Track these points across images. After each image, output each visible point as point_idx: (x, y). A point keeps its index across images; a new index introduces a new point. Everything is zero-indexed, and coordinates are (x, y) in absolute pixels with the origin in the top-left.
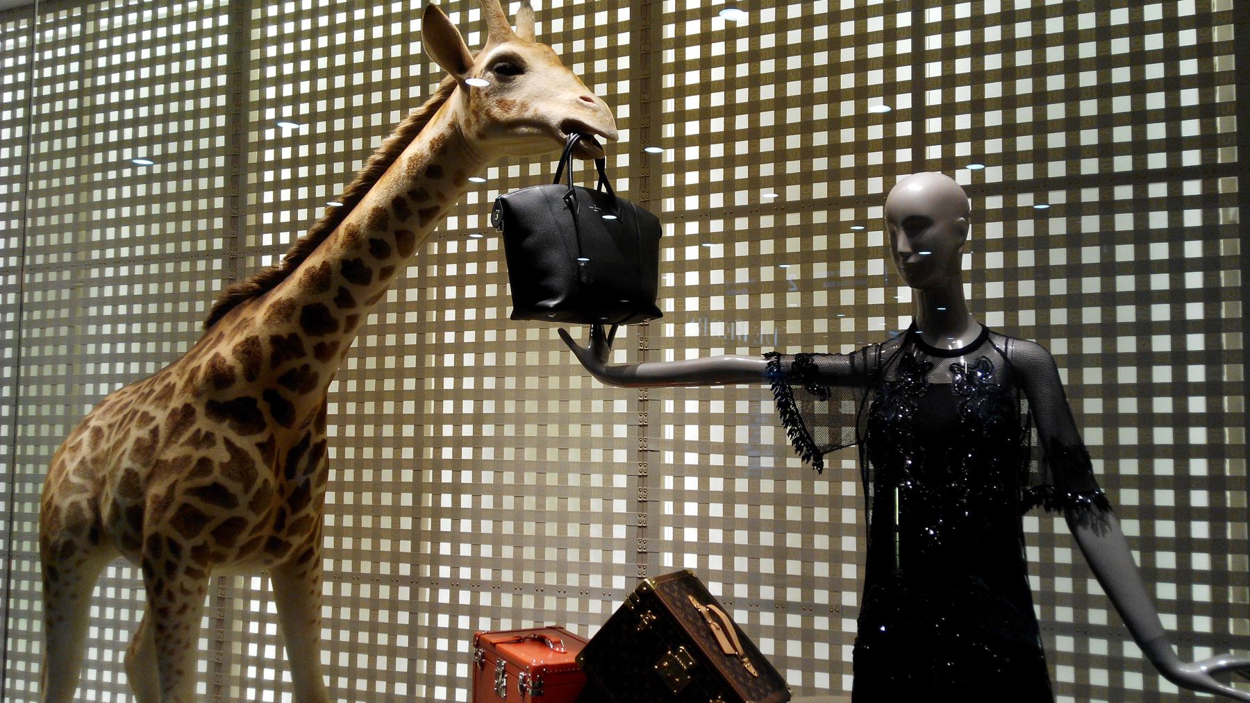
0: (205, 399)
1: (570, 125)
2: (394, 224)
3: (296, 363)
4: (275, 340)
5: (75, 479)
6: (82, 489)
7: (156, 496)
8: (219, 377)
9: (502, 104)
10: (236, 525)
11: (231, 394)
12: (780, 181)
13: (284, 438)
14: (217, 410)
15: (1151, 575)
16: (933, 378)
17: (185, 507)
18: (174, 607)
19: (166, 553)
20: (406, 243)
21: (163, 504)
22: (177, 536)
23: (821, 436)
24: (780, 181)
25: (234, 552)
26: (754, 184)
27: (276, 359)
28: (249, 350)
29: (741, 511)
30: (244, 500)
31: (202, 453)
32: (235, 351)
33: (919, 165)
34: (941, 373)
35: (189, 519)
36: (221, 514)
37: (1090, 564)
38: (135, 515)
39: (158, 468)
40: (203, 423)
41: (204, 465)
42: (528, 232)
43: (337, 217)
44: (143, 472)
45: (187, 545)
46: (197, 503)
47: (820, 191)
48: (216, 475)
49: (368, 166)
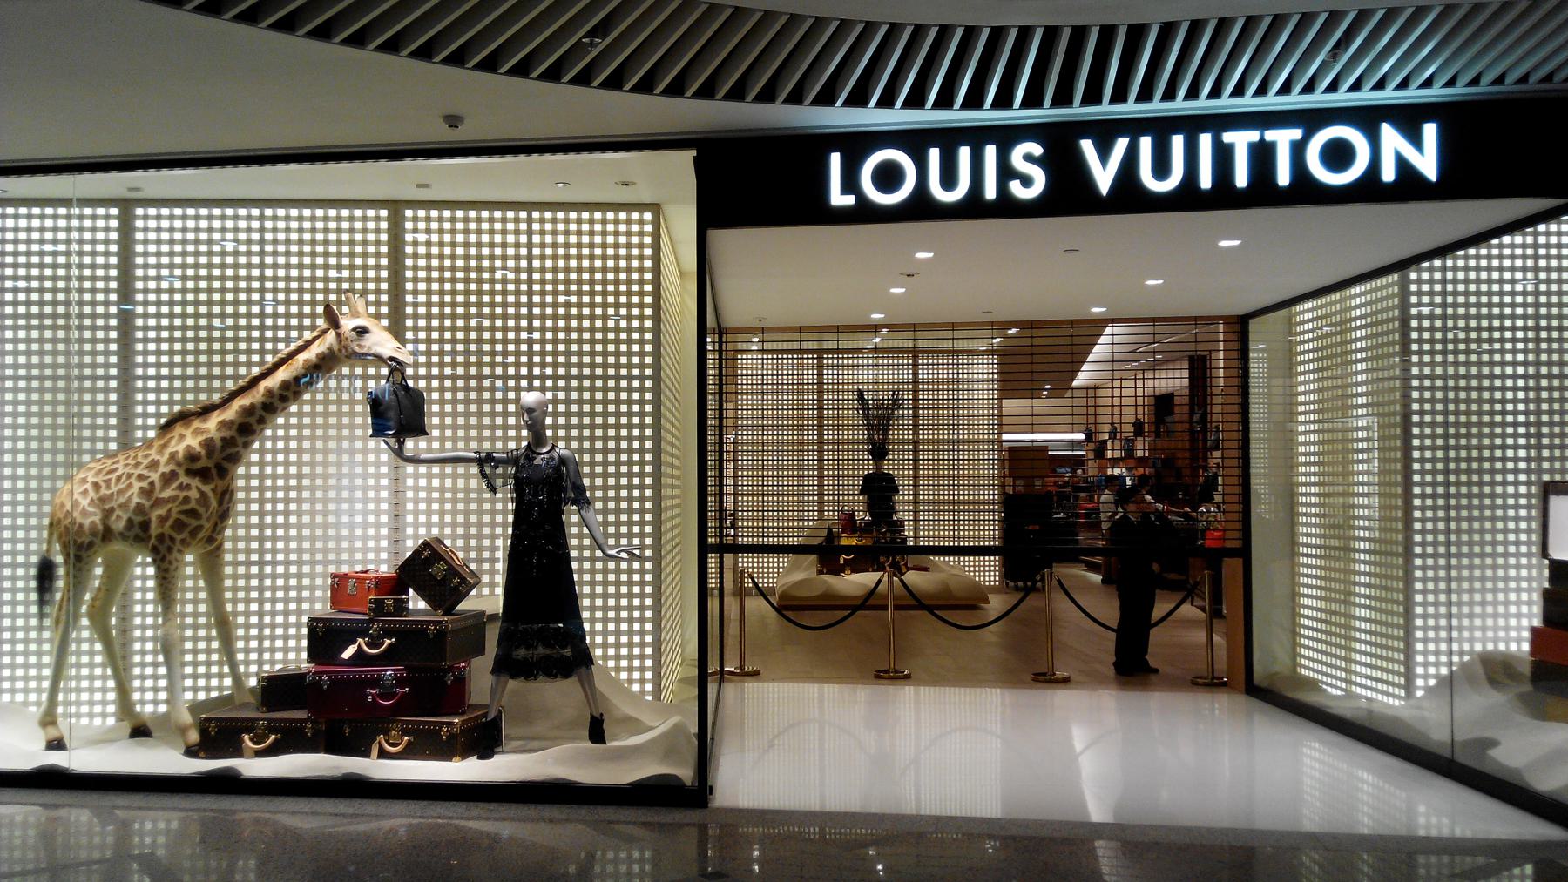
0: (184, 467)
1: (392, 359)
2: (293, 388)
3: (233, 450)
4: (223, 439)
5: (90, 509)
6: (94, 514)
7: (160, 516)
8: (192, 457)
9: (359, 346)
10: (200, 528)
11: (198, 465)
12: (454, 365)
13: (221, 484)
14: (190, 472)
15: (607, 535)
16: (535, 462)
17: (178, 519)
18: (172, 568)
19: (168, 542)
20: (297, 395)
21: (163, 520)
22: (174, 534)
23: (499, 482)
24: (454, 365)
25: (194, 543)
26: (442, 365)
27: (223, 448)
28: (208, 444)
29: (448, 518)
30: (205, 516)
31: (184, 494)
32: (200, 444)
33: (531, 388)
34: (538, 461)
35: (179, 526)
36: (194, 523)
37: (584, 522)
38: (145, 526)
39: (159, 502)
40: (183, 479)
41: (186, 500)
42: (380, 405)
43: (255, 381)
44: (147, 504)
45: (178, 538)
46: (182, 517)
47: (473, 371)
48: (193, 505)
49: (276, 360)
